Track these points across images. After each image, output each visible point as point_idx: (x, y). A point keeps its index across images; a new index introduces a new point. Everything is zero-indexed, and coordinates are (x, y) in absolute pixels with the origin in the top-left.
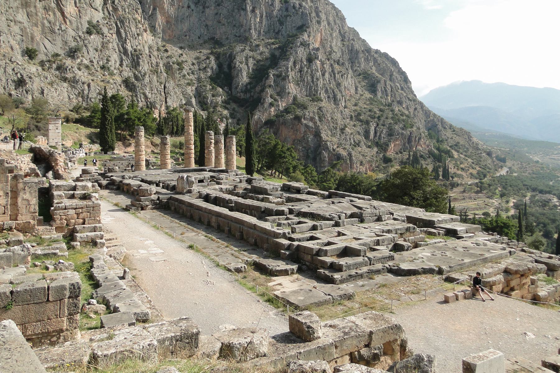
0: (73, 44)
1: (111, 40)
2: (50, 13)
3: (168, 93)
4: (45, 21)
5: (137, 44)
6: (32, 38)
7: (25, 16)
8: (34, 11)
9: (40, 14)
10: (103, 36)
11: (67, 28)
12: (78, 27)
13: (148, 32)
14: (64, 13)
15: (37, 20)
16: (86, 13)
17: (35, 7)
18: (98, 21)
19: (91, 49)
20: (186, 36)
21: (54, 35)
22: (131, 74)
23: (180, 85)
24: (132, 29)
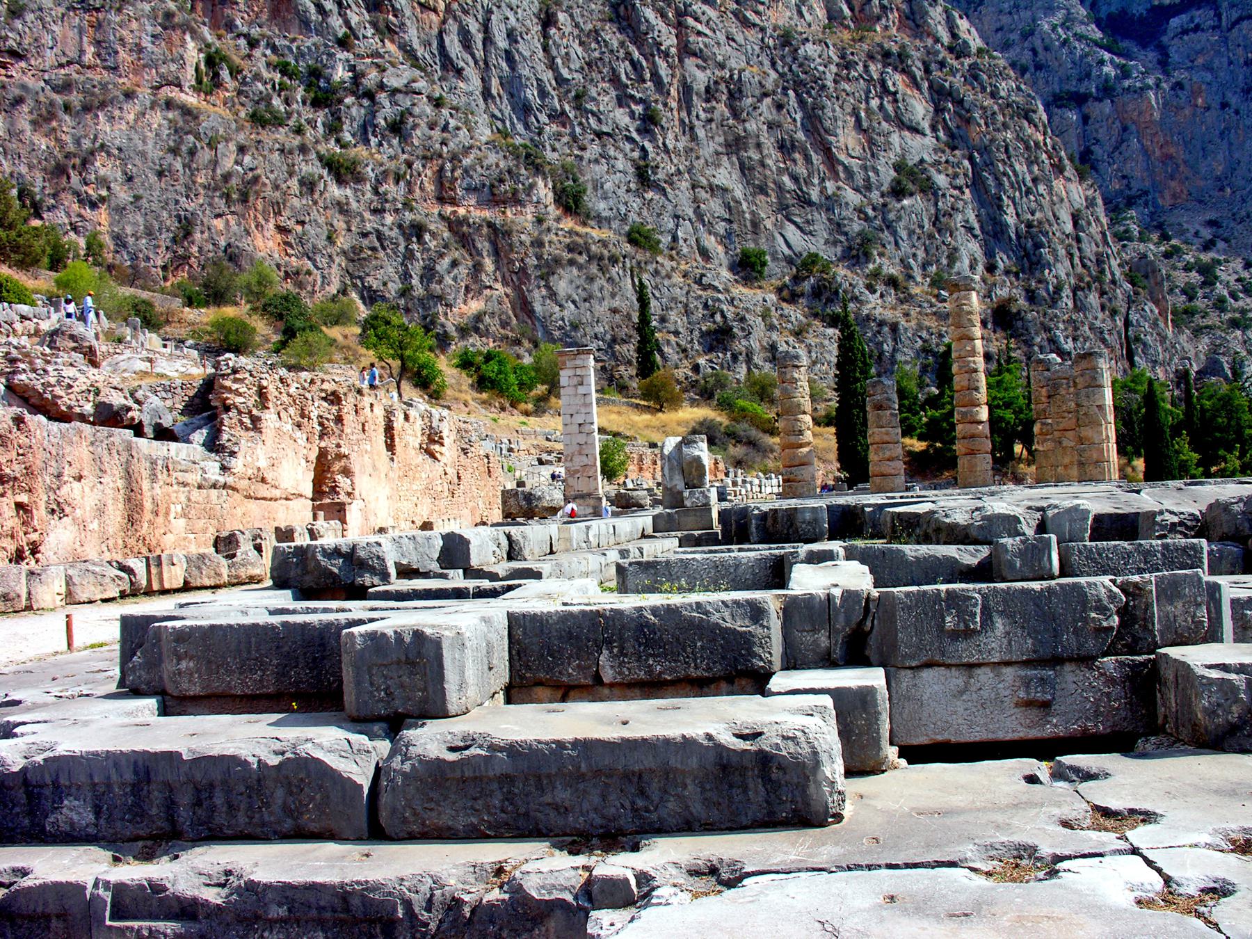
0: (856, 226)
1: (960, 205)
2: (797, 156)
3: (1137, 339)
4: (786, 179)
5: (1033, 205)
6: (756, 224)
7: (736, 174)
8: (755, 156)
9: (769, 162)
10: (935, 194)
11: (839, 188)
12: (867, 180)
13: (1069, 171)
14: (829, 149)
15: (765, 177)
16: (890, 143)
17: (759, 146)
18: (922, 161)
19: (903, 234)
20: (1222, 189)
21: (808, 209)
22: (1018, 293)
23: (1206, 327)
24: (1017, 167)
